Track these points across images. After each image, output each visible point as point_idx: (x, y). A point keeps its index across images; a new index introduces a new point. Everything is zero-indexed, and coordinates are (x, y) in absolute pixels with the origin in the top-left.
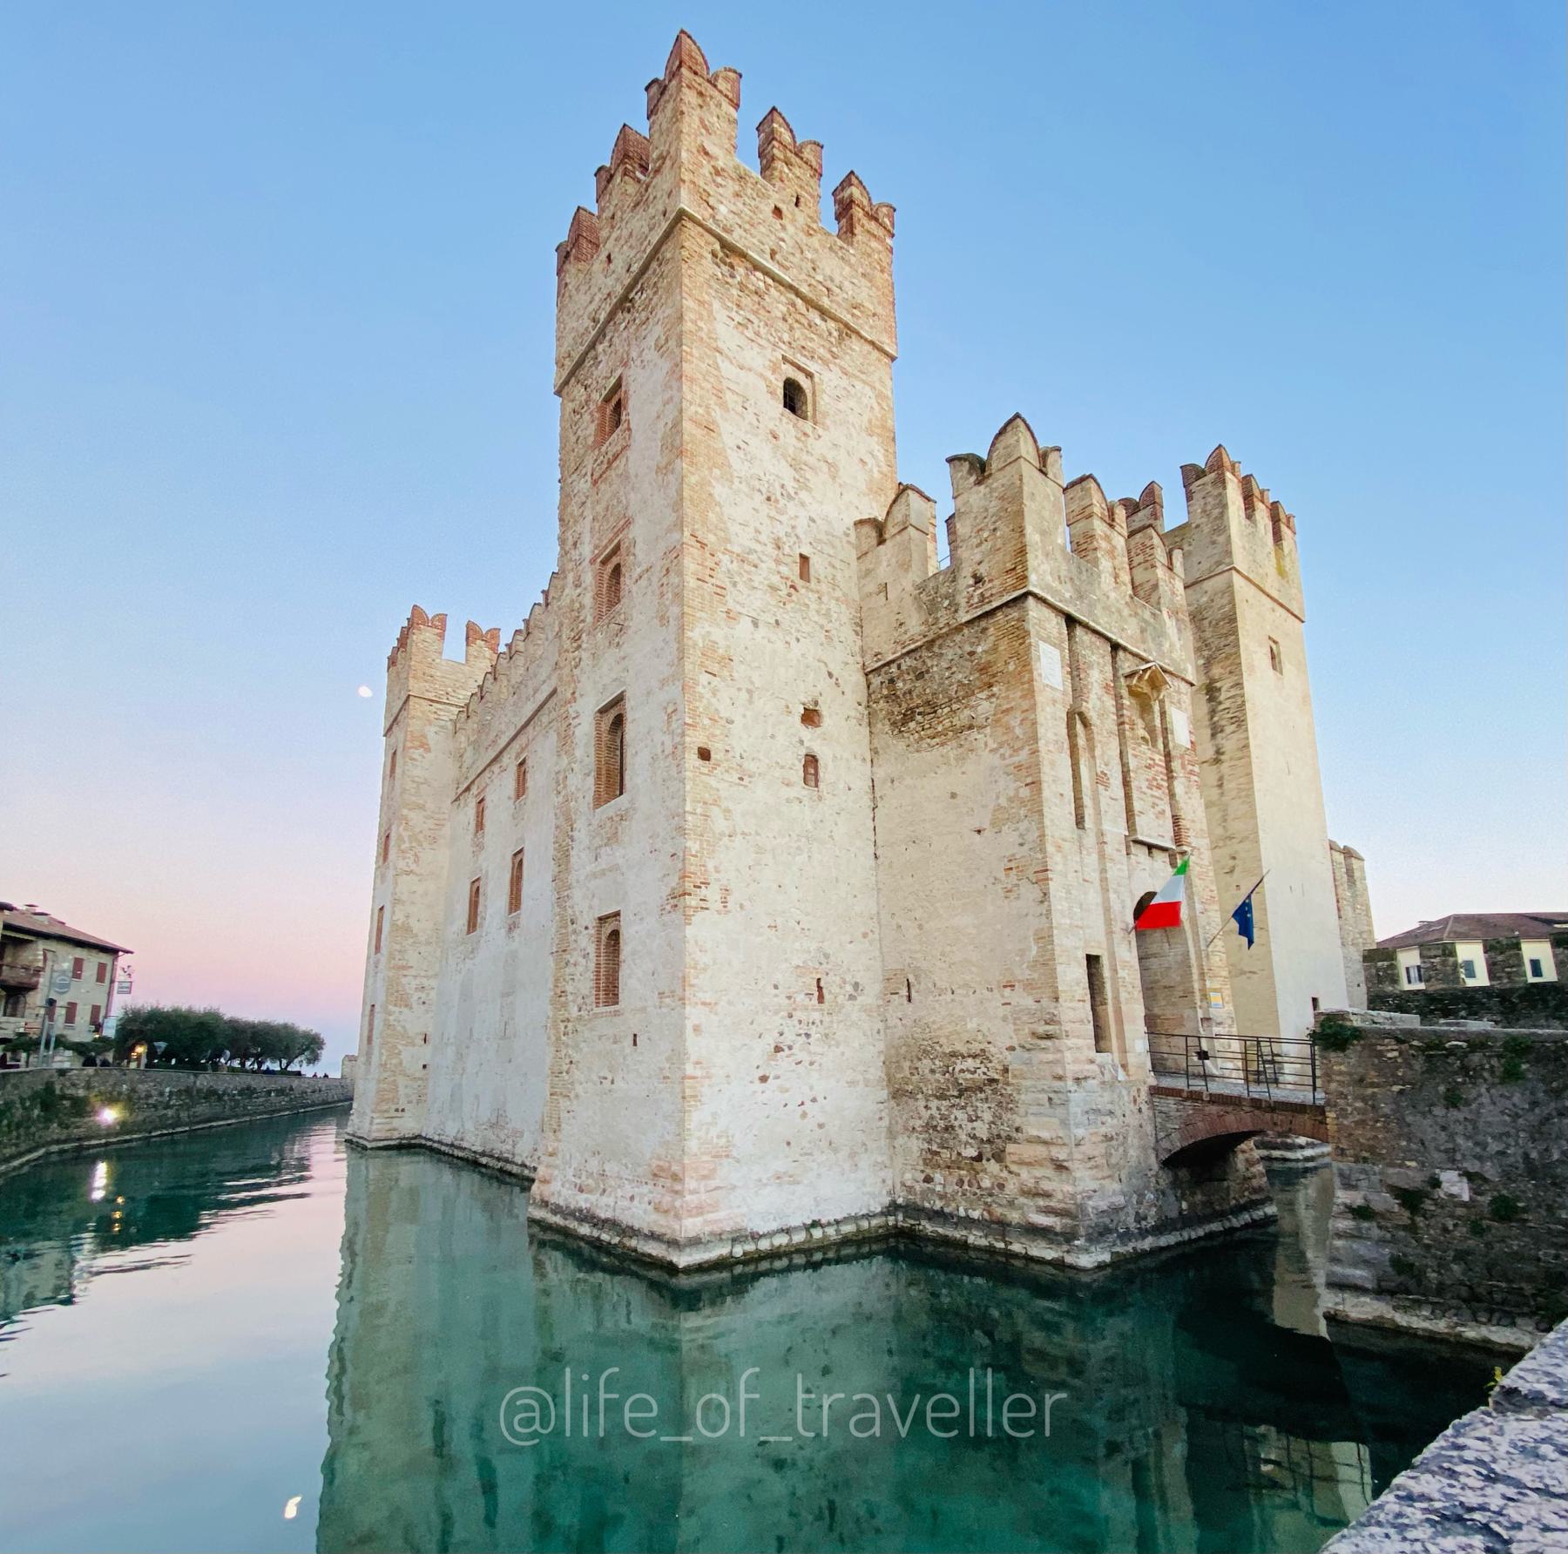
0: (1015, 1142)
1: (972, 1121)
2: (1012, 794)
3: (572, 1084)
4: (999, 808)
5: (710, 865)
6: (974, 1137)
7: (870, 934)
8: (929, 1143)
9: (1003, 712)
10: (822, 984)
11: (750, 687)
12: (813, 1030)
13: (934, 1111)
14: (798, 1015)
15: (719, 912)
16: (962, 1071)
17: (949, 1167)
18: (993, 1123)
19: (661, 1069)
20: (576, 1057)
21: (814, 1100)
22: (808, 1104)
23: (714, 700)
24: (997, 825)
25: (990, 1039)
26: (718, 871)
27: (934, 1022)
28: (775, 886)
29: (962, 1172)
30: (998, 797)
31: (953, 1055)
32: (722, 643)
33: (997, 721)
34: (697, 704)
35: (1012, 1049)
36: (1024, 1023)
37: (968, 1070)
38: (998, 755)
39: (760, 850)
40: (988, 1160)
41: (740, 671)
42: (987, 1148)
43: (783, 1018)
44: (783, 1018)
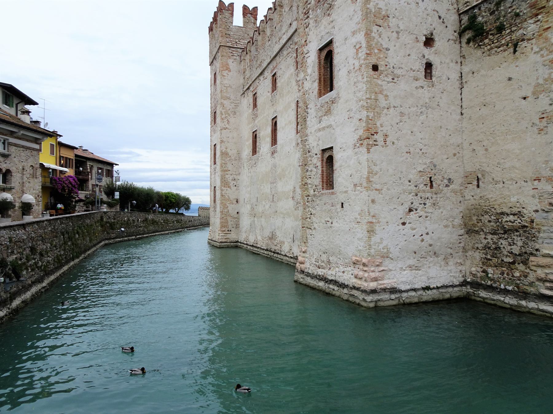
0: (535, 255)
1: (511, 245)
2: (546, 76)
3: (312, 223)
4: (538, 85)
5: (378, 124)
6: (512, 253)
7: (458, 155)
8: (486, 254)
9: (544, 30)
10: (432, 179)
11: (398, 30)
12: (427, 202)
13: (489, 240)
14: (419, 194)
15: (383, 146)
16: (507, 221)
17: (496, 266)
18: (523, 246)
19: (356, 219)
20: (313, 212)
21: (427, 234)
22: (424, 235)
23: (380, 40)
24: (536, 95)
25: (523, 206)
26: (382, 127)
27: (492, 198)
28: (410, 132)
29: (503, 269)
30: (537, 79)
31: (502, 213)
32: (384, 8)
33: (540, 35)
34: (372, 43)
35: (537, 211)
36: (545, 198)
37: (510, 221)
38: (539, 55)
39: (402, 114)
40: (519, 264)
41: (393, 22)
42: (519, 258)
43: (413, 196)
44: (413, 196)
